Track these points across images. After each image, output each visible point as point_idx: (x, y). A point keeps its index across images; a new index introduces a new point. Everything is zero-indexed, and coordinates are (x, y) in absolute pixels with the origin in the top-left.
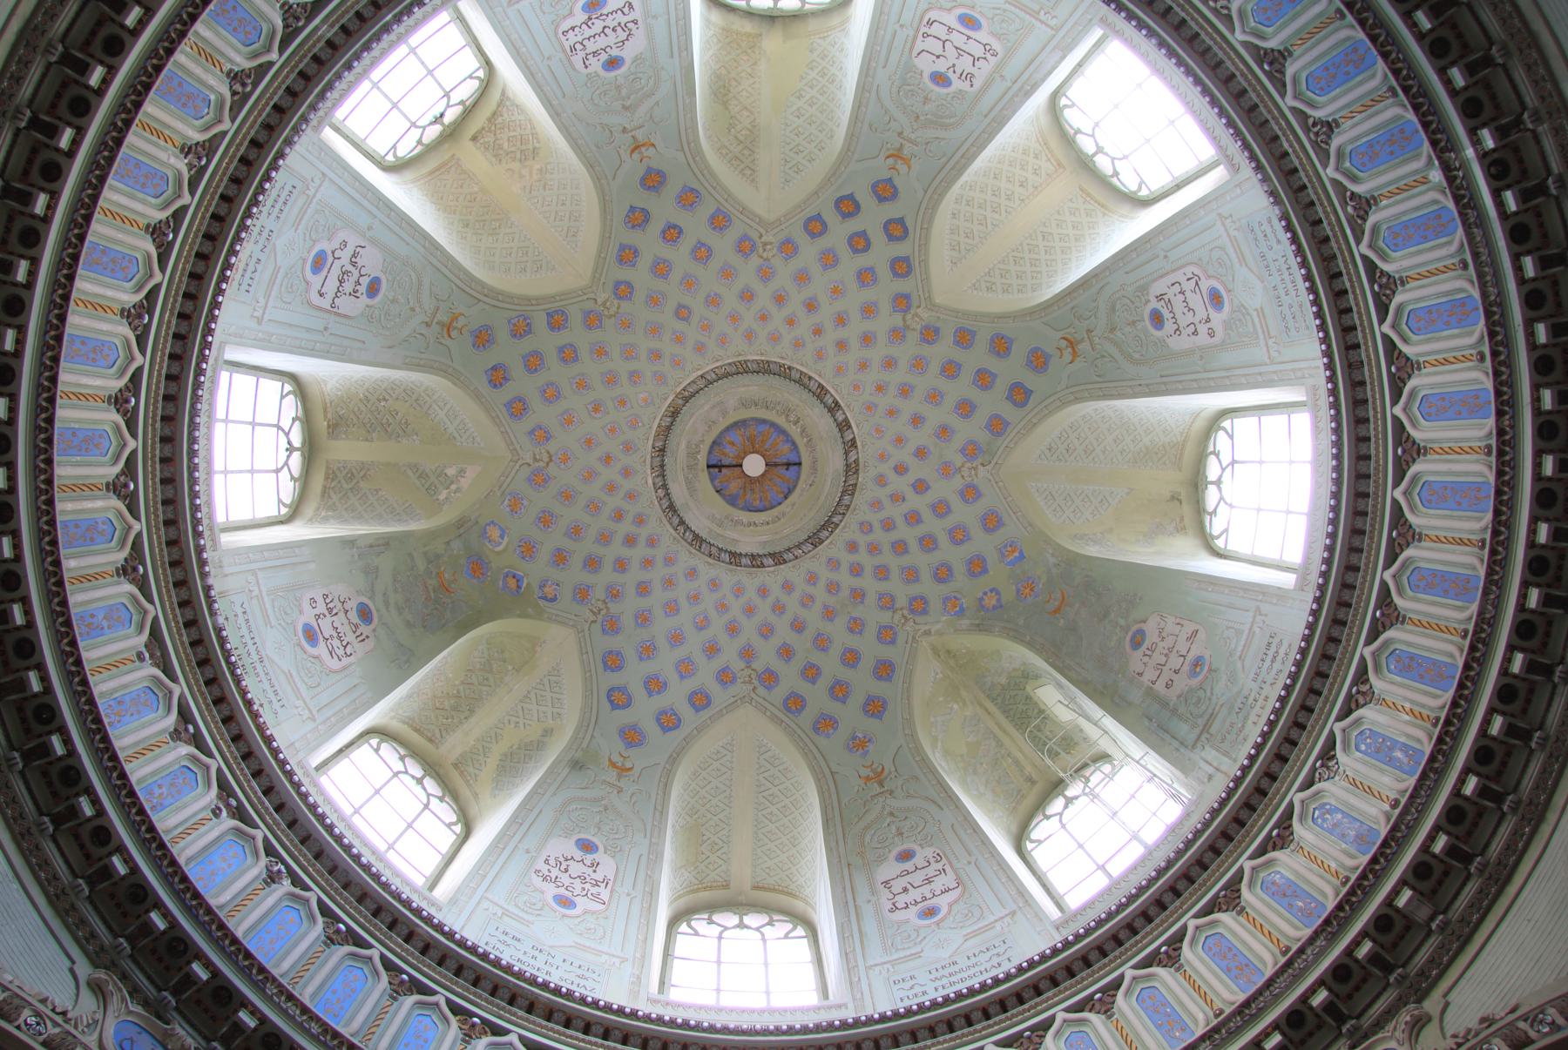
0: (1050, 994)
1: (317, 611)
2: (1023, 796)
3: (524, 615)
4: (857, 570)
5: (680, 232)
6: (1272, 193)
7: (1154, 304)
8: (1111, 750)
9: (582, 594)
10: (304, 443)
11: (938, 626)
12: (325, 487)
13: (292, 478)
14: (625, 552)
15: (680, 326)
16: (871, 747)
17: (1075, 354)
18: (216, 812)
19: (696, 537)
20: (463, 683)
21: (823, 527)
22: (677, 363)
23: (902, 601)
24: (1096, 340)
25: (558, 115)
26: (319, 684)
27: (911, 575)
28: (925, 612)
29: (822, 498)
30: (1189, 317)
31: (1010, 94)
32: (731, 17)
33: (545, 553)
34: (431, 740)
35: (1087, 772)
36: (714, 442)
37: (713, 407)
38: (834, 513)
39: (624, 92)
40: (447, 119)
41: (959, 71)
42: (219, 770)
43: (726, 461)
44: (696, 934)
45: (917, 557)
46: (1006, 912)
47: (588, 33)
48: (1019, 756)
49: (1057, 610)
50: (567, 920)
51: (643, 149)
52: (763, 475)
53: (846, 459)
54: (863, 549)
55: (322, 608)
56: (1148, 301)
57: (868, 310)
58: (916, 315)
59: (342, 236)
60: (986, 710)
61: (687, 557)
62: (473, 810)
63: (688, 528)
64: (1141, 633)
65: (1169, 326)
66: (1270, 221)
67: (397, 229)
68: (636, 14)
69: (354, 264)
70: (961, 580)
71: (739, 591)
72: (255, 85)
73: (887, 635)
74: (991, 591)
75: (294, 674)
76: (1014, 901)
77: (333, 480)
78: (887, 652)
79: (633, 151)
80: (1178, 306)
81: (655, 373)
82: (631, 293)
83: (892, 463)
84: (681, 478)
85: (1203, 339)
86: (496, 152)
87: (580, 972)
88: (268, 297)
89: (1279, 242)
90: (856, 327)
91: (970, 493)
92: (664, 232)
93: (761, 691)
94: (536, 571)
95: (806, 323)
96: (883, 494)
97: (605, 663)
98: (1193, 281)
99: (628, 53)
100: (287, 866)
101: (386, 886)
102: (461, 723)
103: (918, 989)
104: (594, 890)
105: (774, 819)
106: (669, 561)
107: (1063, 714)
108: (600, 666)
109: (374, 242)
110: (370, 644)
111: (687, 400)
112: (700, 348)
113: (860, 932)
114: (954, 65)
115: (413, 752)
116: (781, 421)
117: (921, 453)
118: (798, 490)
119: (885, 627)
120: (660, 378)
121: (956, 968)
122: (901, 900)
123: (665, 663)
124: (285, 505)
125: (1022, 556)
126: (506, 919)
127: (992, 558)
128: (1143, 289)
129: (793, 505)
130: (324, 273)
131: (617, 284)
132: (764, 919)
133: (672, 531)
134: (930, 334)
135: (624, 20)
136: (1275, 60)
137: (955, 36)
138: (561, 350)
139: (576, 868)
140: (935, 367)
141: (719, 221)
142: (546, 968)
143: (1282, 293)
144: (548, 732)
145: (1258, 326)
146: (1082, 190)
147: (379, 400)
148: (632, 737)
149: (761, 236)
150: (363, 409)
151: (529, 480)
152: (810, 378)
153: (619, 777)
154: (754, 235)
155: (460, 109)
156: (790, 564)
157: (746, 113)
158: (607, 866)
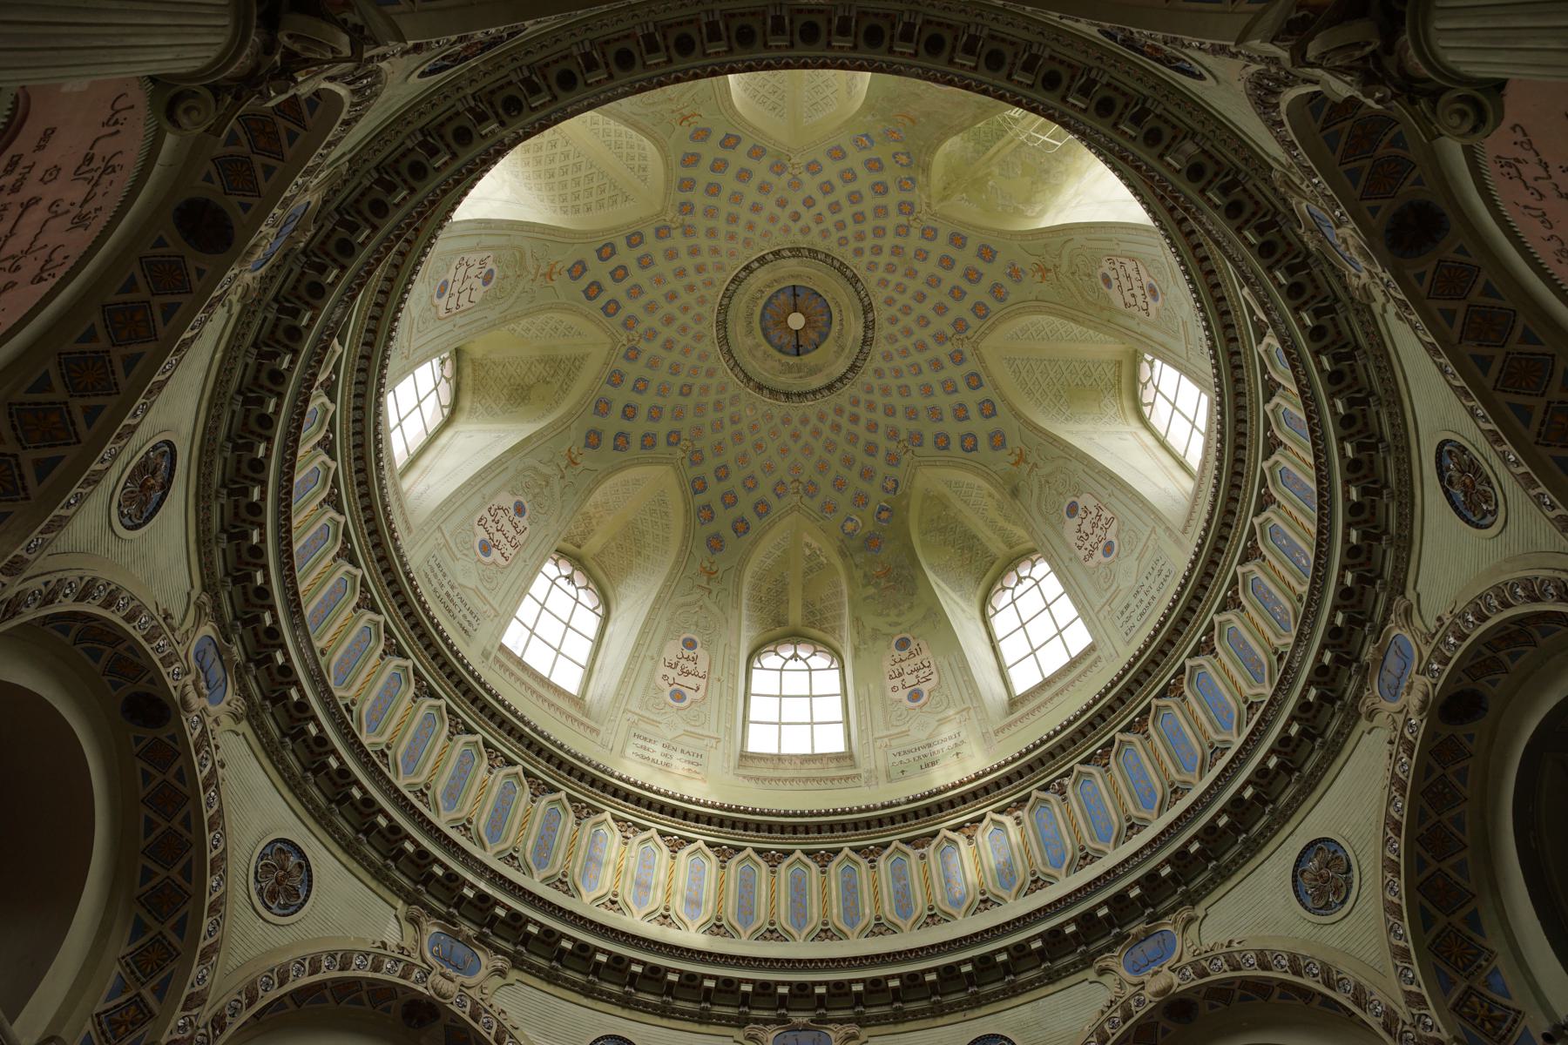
5: (627, 406)
9: (893, 460)
13: (814, 654)
14: (863, 422)
15: (696, 390)
16: (1019, 266)
17: (693, 115)
21: (843, 274)
22: (722, 389)
23: (903, 220)
27: (881, 211)
32: (463, 386)
33: (864, 486)
36: (780, 350)
37: (754, 356)
39: (537, 490)
47: (504, 541)
49: (912, 121)
55: (897, 682)
57: (671, 255)
58: (671, 221)
59: (660, 682)
61: (866, 376)
69: (676, 665)
71: (892, 339)
72: (581, 801)
73: (929, 234)
78: (943, 237)
79: (576, 464)
81: (731, 404)
83: (791, 223)
87: (1156, 572)
88: (701, 737)
92: (629, 419)
93: (969, 333)
94: (877, 497)
95: (686, 298)
96: (815, 230)
97: (944, 448)
99: (508, 501)
100: (1057, 778)
104: (1103, 521)
106: (870, 390)
108: (945, 452)
110: (923, 645)
111: (750, 379)
112: (710, 373)
115: (1000, 575)
116: (762, 303)
117: (782, 203)
118: (816, 288)
120: (735, 400)
125: (866, 136)
130: (683, 689)
131: (669, 444)
135: (490, 519)
138: (720, 479)
141: (616, 379)
148: (998, 441)
151: (812, 497)
152: (727, 289)
154: (623, 350)
157: (533, 369)
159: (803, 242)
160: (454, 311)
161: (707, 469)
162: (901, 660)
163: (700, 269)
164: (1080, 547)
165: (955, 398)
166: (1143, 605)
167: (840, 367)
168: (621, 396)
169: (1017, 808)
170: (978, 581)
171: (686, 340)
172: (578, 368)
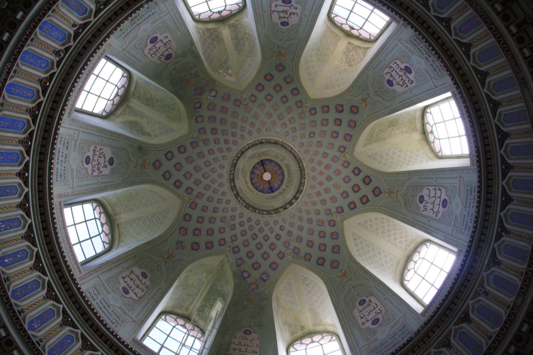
0: (106, 346)
1: (163, 40)
2: (181, 309)
3: (188, 113)
4: (241, 224)
5: (340, 125)
6: (418, 331)
7: (367, 300)
8: (207, 333)
10: (223, 16)
11: (231, 259)
12: (210, 29)
15: (307, 135)
18: (74, 25)
19: (235, 164)
20: (157, 99)
21: (253, 207)
23: (235, 243)
24: (348, 283)
25: (366, 69)
26: (137, 48)
28: (235, 253)
29: (263, 204)
30: (366, 314)
31: (424, 226)
34: (133, 94)
35: (196, 329)
36: (270, 161)
38: (259, 210)
39: (381, 90)
40: (353, 31)
41: (426, 205)
42: (90, 22)
43: (264, 166)
44: (94, 210)
45: (253, 244)
46: (134, 318)
47: (398, 71)
48: (195, 303)
50: (81, 164)
51: (364, 103)
52: (265, 181)
53: (279, 208)
54: (250, 224)
55: (165, 41)
56: (367, 297)
58: (337, 216)
60: (207, 285)
61: (227, 164)
62: (113, 117)
63: (237, 160)
64: (250, 333)
65: (361, 308)
66: (409, 333)
67: (308, 26)
68: (410, 86)
69: (290, 14)
70: (249, 262)
74: (249, 274)
75: (138, 38)
76: (139, 320)
77: (214, 31)
78: (216, 245)
79: (362, 99)
80: (369, 309)
81: (287, 132)
82: (313, 115)
83: (283, 224)
84: (255, 152)
85: (360, 321)
86: (347, 52)
87: (63, 174)
89: (402, 339)
90: (326, 196)
91: (280, 255)
93: (188, 205)
94: (205, 112)
96: (271, 224)
98: (380, 311)
99: (396, 87)
101: (69, 95)
102: (143, 103)
103: (95, 297)
104: (96, 169)
105: (144, 224)
107: (213, 314)
108: (178, 146)
109: (301, 19)
110: (158, 62)
111: (282, 146)
113: (111, 269)
114: (428, 203)
116: (285, 181)
117: (290, 233)
118: (263, 194)
119: (225, 241)
121: (107, 307)
122: (127, 279)
123: (188, 168)
124: (199, 17)
125: (265, 281)
126: (74, 141)
127: (261, 270)
128: (372, 294)
129: (258, 194)
131: (315, 109)
132: (108, 232)
133: (235, 155)
134: (332, 223)
135: (407, 82)
136: (466, 318)
137: (438, 200)
139: (102, 160)
140: (321, 229)
142: (60, 162)
143: (385, 346)
144: (149, 134)
145: (371, 340)
146: (400, 260)
147: (247, 38)
148: (157, 165)
149: (347, 154)
150: (242, 34)
152: (304, 186)
153: (141, 165)
154: (347, 151)
155: (358, 34)
156: (236, 200)
157: (388, 135)
158: (106, 171)
159: (275, 217)
160: (437, 188)
161: (292, 100)
162: (167, 50)
163: (319, 194)
164: (101, 149)
165: (183, 172)
166: (60, 156)
167: (241, 164)
168: (344, 129)
169: (78, 29)
170: (137, 85)
171: (318, 158)
172: (367, 140)
